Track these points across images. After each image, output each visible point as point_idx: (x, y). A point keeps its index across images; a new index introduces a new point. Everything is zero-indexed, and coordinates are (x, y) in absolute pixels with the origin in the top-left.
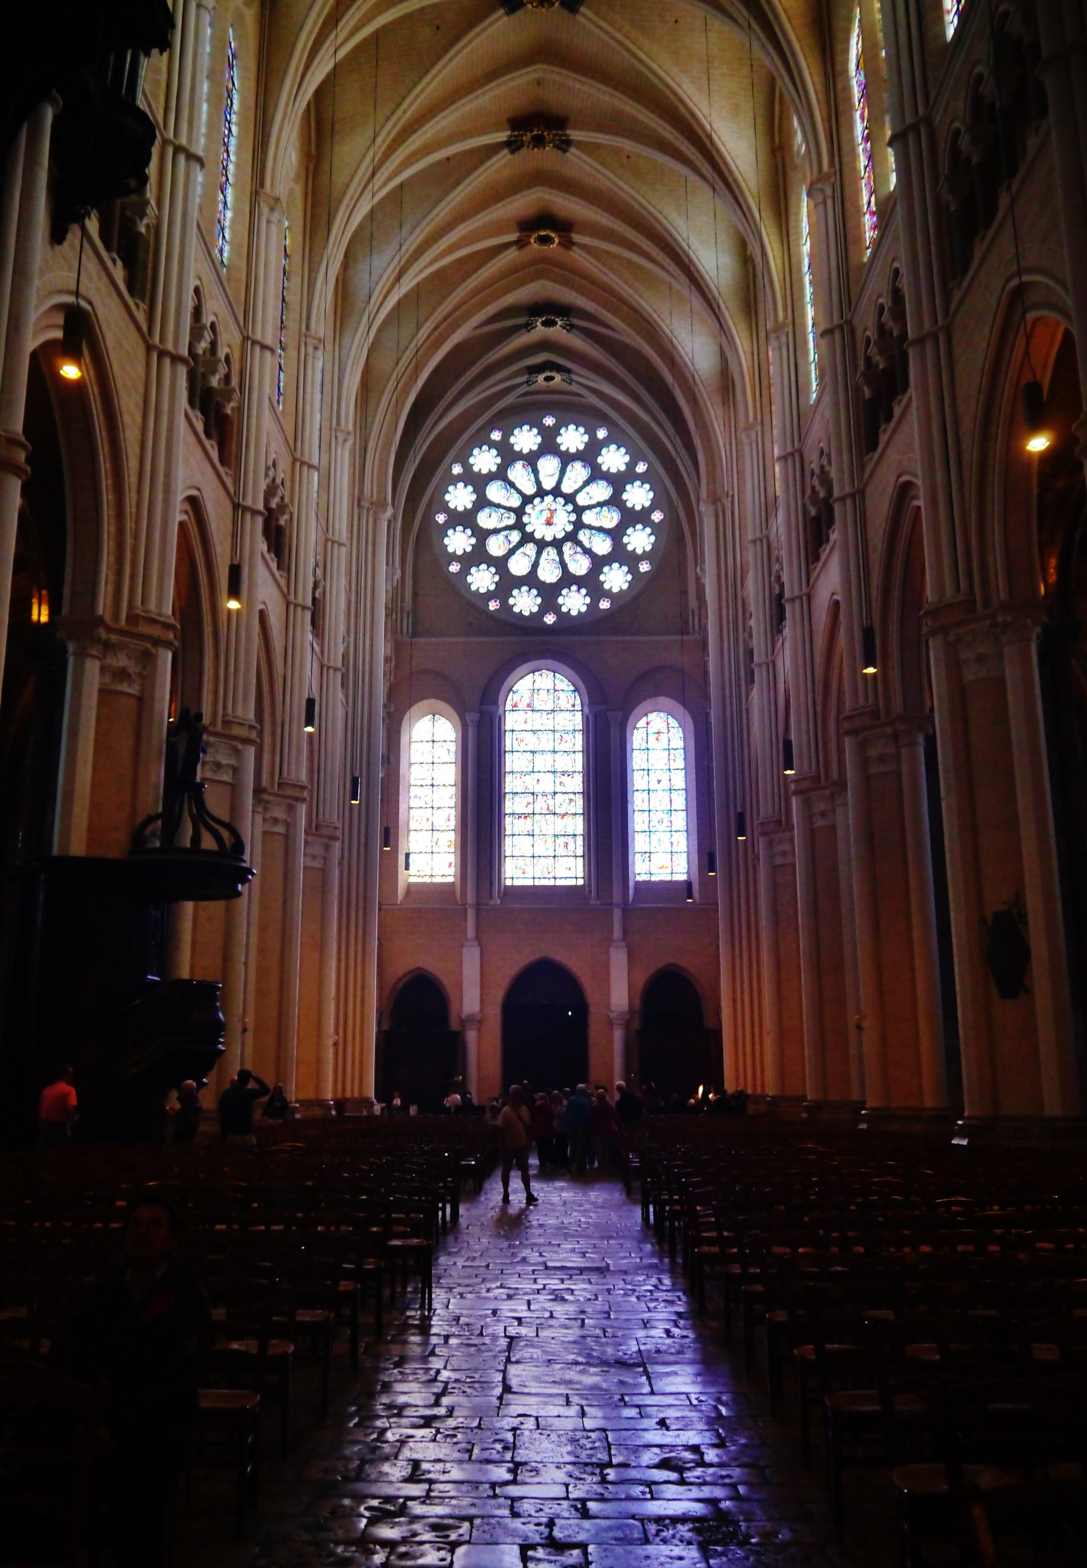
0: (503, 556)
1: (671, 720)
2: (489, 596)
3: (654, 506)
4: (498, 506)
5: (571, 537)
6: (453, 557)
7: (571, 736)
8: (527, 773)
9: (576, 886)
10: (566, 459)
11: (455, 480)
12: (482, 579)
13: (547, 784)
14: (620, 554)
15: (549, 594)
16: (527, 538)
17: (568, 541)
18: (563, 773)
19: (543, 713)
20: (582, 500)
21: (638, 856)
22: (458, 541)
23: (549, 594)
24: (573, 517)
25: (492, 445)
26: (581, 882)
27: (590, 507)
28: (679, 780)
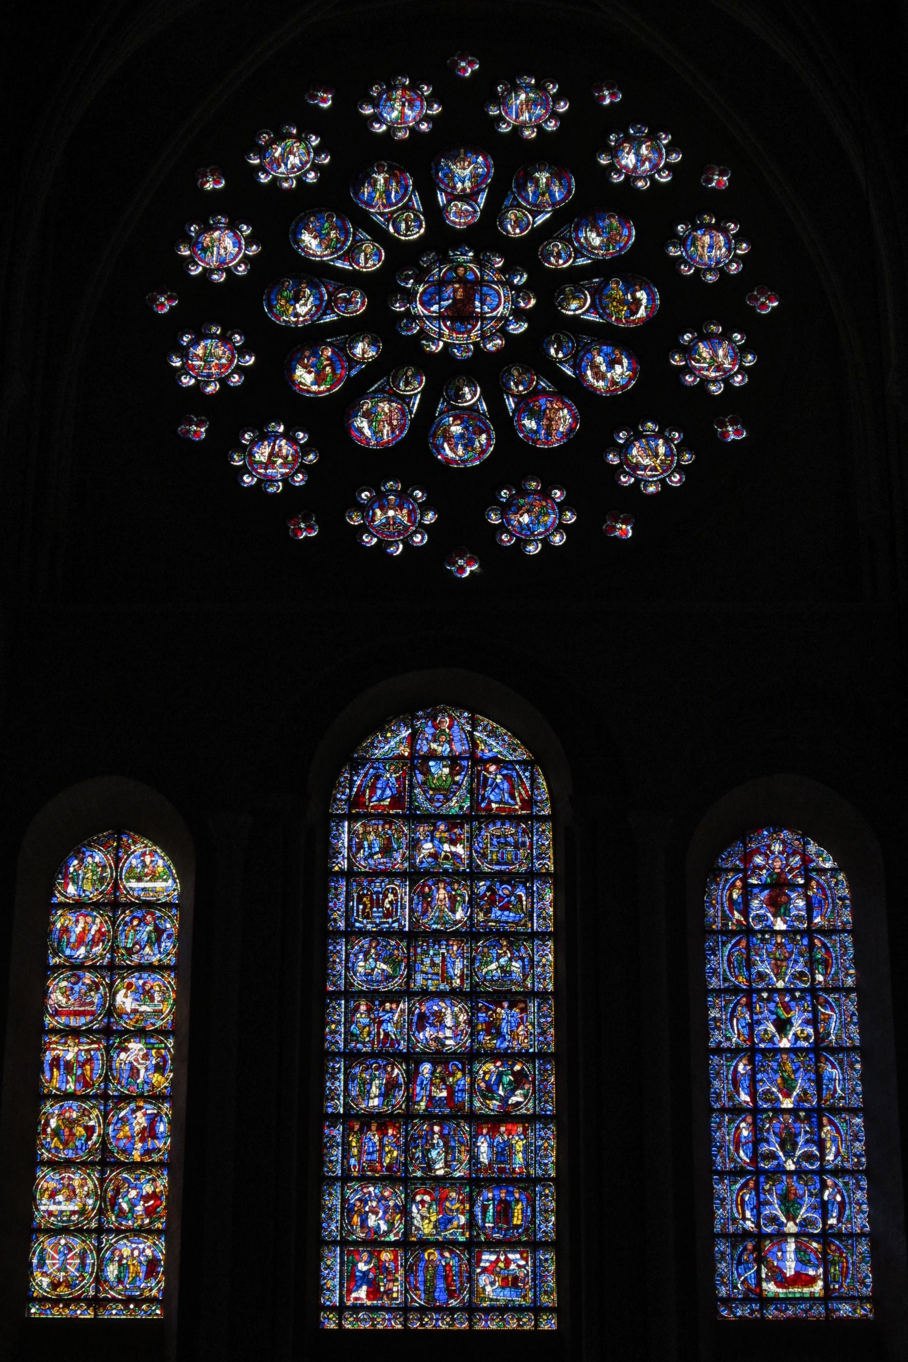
1: (812, 848)
7: (520, 892)
8: (394, 997)
9: (537, 1334)
12: (273, 459)
13: (450, 1025)
14: (661, 397)
15: (462, 500)
18: (498, 997)
19: (443, 842)
21: (722, 1246)
22: (211, 360)
23: (462, 500)
25: (310, 122)
26: (549, 1324)
27: (575, 276)
28: (840, 1022)
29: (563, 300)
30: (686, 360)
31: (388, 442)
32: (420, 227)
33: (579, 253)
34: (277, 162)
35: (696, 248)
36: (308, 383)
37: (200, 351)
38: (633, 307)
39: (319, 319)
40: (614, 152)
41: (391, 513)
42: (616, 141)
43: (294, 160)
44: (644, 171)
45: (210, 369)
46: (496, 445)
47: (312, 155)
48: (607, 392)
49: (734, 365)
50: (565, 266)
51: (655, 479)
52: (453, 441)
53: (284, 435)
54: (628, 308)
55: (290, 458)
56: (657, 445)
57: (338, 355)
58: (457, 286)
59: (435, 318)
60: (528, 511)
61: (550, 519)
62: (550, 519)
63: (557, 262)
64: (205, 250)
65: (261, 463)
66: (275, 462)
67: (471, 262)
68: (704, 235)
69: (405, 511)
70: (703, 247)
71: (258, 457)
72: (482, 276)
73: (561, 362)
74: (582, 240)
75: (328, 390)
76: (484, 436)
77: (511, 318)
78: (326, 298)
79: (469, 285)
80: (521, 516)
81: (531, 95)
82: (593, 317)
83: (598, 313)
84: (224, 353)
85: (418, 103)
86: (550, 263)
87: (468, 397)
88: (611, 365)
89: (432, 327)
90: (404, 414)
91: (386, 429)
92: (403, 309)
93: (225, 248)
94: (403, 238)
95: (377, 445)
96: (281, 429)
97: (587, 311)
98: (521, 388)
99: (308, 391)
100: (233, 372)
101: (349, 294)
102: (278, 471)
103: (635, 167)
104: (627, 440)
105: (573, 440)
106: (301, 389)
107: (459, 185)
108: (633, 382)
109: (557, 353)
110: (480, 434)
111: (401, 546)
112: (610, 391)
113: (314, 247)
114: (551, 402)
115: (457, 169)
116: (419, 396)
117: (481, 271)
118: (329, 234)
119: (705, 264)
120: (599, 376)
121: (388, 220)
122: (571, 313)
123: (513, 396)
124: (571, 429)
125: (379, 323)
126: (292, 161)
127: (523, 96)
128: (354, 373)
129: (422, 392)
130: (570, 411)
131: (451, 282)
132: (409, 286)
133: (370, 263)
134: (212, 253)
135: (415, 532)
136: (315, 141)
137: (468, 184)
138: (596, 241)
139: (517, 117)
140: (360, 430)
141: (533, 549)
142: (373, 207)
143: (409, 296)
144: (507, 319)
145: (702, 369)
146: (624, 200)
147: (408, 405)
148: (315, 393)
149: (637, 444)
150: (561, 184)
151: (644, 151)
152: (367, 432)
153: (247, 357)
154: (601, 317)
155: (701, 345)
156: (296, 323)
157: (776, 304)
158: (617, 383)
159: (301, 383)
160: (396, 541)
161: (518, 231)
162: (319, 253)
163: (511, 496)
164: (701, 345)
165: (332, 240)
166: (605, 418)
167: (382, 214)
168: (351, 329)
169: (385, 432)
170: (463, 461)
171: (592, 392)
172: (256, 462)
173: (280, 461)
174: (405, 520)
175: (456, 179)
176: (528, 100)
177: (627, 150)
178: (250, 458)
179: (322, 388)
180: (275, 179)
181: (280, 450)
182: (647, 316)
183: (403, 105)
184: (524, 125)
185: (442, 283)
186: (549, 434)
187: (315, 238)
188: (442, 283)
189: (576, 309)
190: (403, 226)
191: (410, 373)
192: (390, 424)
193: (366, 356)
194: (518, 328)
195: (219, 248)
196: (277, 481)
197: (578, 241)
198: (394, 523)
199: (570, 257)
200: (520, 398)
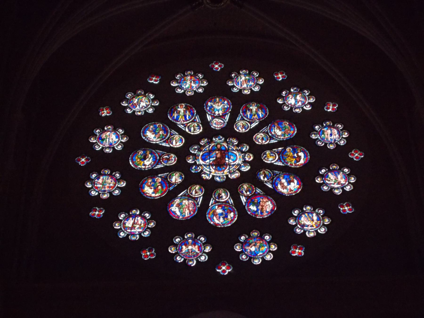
0: (161, 199)
2: (144, 243)
3: (351, 144)
4: (157, 147)
5: (250, 178)
6: (98, 201)
10: (239, 102)
11: (102, 123)
12: (134, 226)
15: (222, 241)
16: (192, 178)
17: (244, 182)
20: (260, 138)
22: (105, 185)
24: (250, 158)
25: (148, 89)
27: (270, 147)
29: (265, 157)
30: (323, 180)
31: (188, 217)
32: (200, 129)
33: (271, 138)
34: (134, 106)
35: (325, 135)
36: (151, 193)
37: (100, 181)
38: (298, 159)
39: (155, 167)
40: (285, 98)
41: (190, 247)
42: (286, 94)
43: (143, 104)
44: (299, 106)
45: (105, 188)
46: (238, 217)
47: (151, 102)
48: (288, 194)
49: (346, 182)
50: (265, 143)
51: (313, 230)
52: (218, 216)
53: (140, 215)
54: (296, 160)
55: (142, 225)
56: (313, 216)
57: (164, 181)
58: (217, 152)
59: (208, 165)
60: (254, 245)
61: (264, 248)
62: (264, 248)
63: (262, 142)
64: (103, 140)
65: (129, 227)
66: (135, 227)
67: (223, 142)
68: (328, 129)
69: (197, 246)
70: (327, 135)
71: (127, 225)
72: (228, 148)
73: (266, 182)
74: (273, 133)
75: (160, 196)
76: (232, 214)
77: (242, 165)
78: (158, 158)
79: (223, 152)
80: (251, 247)
81: (247, 78)
82: (280, 164)
83: (282, 162)
84: (112, 181)
85: (197, 82)
86: (259, 142)
87: (224, 197)
88: (289, 183)
89: (206, 170)
90: (195, 205)
91: (187, 211)
92: (193, 162)
93: (112, 139)
94: (192, 134)
95: (183, 218)
96: (138, 213)
97: (277, 161)
98: (248, 193)
99: (150, 197)
100: (116, 189)
101: (169, 156)
102: (137, 230)
103: (295, 104)
104: (298, 214)
105: (273, 214)
106: (147, 196)
107: (217, 113)
108: (300, 190)
109: (264, 179)
110: (230, 213)
111: (195, 262)
112: (289, 194)
113: (152, 138)
114: (262, 199)
115: (216, 106)
116: (201, 198)
117: (228, 146)
118: (159, 132)
119: (329, 141)
120: (283, 187)
121: (185, 127)
122: (270, 162)
123: (245, 196)
124: (272, 210)
125: (182, 166)
126: (142, 104)
127: (243, 78)
128: (171, 188)
129: (203, 196)
130: (272, 202)
131: (215, 150)
132: (196, 153)
133: (178, 144)
134: (106, 141)
135: (202, 255)
136: (152, 96)
137: (221, 112)
138: (279, 133)
139: (241, 86)
140: (174, 212)
141: (257, 262)
142: (179, 122)
143: (195, 156)
144: (240, 165)
145: (331, 184)
146: (291, 117)
147: (197, 201)
148: (153, 197)
149: (303, 216)
150: (262, 111)
151: (298, 97)
152: (178, 213)
153: (122, 183)
154: (283, 163)
155: (329, 174)
156: (145, 168)
157: (362, 157)
158: (292, 191)
159: (147, 193)
160: (193, 260)
161: (244, 130)
162: (154, 140)
163: (246, 239)
164: (329, 174)
165: (160, 135)
166: (286, 205)
167: (183, 124)
168: (171, 169)
169: (186, 213)
170: (223, 225)
171: (281, 195)
172: (126, 227)
173: (138, 226)
174: (197, 250)
175: (215, 110)
176: (245, 80)
177: (291, 97)
178: (124, 225)
179: (157, 195)
180: (134, 112)
181: (138, 222)
182: (304, 163)
183: (191, 82)
184: (244, 89)
185: (210, 151)
186: (262, 213)
187: (153, 134)
188: (210, 151)
189: (272, 161)
190: (192, 129)
191: (197, 188)
192: (189, 209)
193: (177, 181)
194: (246, 169)
195: (109, 139)
196: (136, 235)
197: (271, 133)
198: (192, 252)
199: (268, 139)
200: (248, 197)
